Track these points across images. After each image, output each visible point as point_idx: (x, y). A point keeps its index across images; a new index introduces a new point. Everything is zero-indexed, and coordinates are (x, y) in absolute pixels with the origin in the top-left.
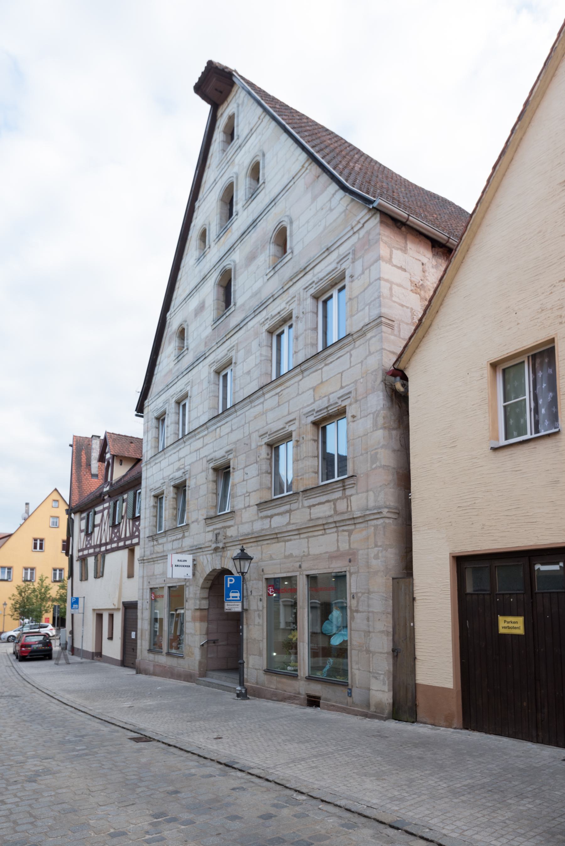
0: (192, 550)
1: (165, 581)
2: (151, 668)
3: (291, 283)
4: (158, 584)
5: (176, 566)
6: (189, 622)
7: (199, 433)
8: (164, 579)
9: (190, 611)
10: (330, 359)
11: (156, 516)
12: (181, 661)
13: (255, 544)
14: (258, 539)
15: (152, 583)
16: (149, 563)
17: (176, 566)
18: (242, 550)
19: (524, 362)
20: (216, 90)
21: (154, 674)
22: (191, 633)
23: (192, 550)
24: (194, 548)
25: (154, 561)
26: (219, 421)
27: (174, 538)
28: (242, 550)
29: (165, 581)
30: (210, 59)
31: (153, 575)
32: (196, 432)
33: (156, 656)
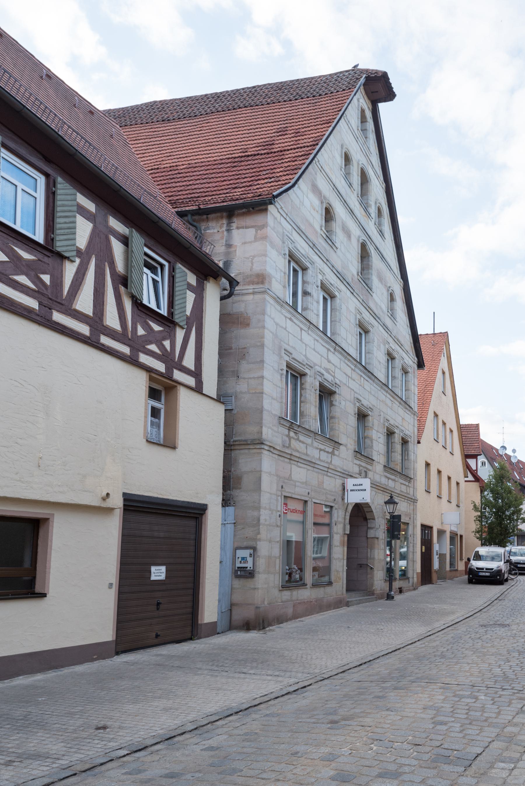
0: (343, 473)
1: (309, 494)
2: (290, 611)
3: (325, 260)
4: (298, 495)
5: (351, 490)
6: (337, 546)
7: (349, 360)
8: (307, 491)
9: (339, 535)
10: (407, 411)
11: (365, 438)
12: (329, 589)
13: (381, 492)
14: (385, 490)
15: (286, 488)
16: (280, 458)
17: (351, 490)
18: (391, 497)
19: (35, 235)
20: (377, 92)
21: (295, 617)
22: (339, 558)
23: (343, 473)
24: (347, 473)
25: (290, 459)
26: (364, 373)
27: (322, 447)
28: (391, 497)
29: (309, 494)
30: (396, 98)
31: (290, 478)
32: (348, 357)
33: (295, 593)
